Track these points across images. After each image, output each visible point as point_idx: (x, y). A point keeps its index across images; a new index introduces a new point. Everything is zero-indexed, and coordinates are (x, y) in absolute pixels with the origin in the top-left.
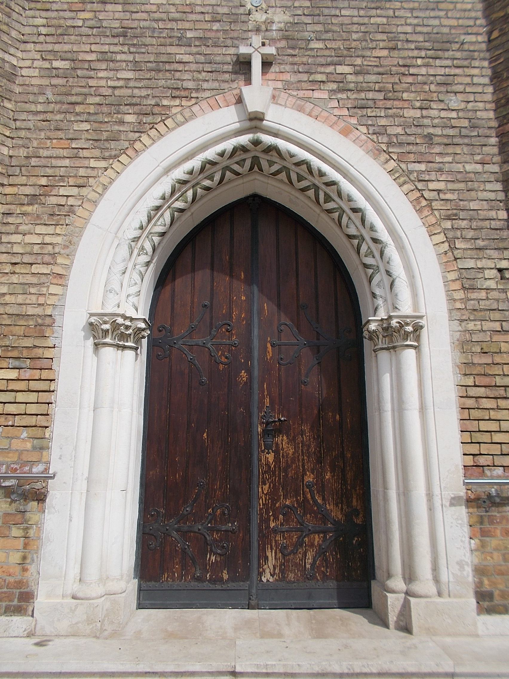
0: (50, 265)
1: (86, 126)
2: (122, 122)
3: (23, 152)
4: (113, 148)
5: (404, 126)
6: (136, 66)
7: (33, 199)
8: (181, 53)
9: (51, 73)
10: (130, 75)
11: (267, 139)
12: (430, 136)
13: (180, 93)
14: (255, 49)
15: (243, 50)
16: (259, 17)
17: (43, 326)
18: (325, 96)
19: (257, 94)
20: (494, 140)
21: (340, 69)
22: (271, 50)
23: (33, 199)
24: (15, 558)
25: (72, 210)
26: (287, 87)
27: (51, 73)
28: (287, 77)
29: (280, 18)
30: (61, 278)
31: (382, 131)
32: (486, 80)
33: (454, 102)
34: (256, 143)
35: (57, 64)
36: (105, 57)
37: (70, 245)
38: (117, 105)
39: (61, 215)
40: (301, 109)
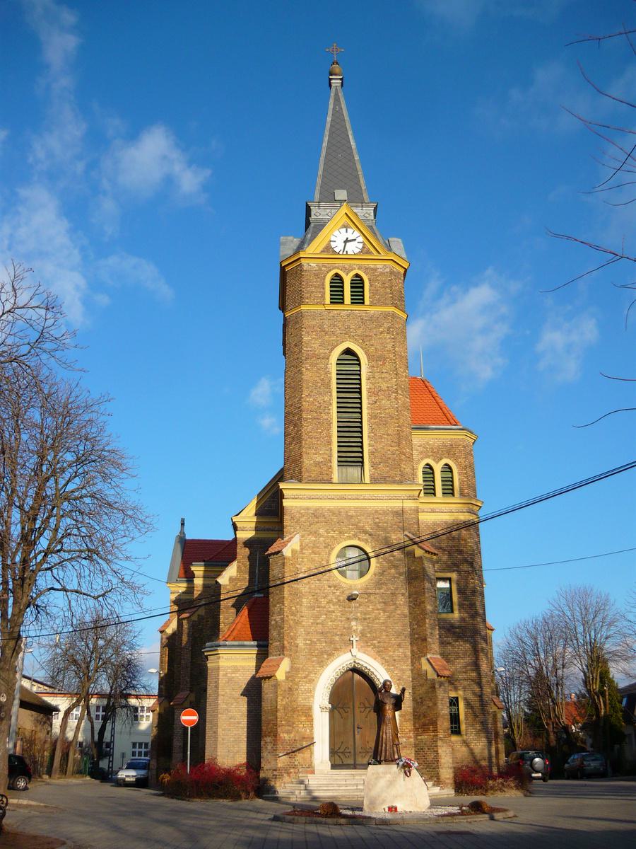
0: (310, 692)
1: (315, 659)
2: (324, 658)
3: (301, 666)
4: (322, 664)
5: (390, 656)
6: (326, 642)
7: (305, 678)
8: (337, 638)
9: (305, 644)
10: (324, 645)
11: (357, 661)
12: (395, 660)
13: (336, 649)
14: (354, 639)
15: (351, 639)
16: (354, 628)
17: (310, 708)
18: (370, 649)
19: (355, 651)
20: (410, 660)
21: (375, 642)
22: (357, 639)
23: (305, 678)
24: (309, 755)
25: (314, 680)
26: (362, 647)
27: (305, 644)
28: (362, 644)
29: (360, 628)
30: (313, 696)
31: (383, 658)
32: (408, 644)
33: (401, 650)
34: (355, 662)
35: (307, 642)
36: (318, 640)
37: (314, 689)
38: (322, 653)
39: (311, 681)
40: (365, 653)
